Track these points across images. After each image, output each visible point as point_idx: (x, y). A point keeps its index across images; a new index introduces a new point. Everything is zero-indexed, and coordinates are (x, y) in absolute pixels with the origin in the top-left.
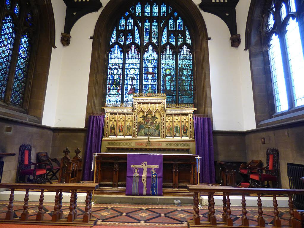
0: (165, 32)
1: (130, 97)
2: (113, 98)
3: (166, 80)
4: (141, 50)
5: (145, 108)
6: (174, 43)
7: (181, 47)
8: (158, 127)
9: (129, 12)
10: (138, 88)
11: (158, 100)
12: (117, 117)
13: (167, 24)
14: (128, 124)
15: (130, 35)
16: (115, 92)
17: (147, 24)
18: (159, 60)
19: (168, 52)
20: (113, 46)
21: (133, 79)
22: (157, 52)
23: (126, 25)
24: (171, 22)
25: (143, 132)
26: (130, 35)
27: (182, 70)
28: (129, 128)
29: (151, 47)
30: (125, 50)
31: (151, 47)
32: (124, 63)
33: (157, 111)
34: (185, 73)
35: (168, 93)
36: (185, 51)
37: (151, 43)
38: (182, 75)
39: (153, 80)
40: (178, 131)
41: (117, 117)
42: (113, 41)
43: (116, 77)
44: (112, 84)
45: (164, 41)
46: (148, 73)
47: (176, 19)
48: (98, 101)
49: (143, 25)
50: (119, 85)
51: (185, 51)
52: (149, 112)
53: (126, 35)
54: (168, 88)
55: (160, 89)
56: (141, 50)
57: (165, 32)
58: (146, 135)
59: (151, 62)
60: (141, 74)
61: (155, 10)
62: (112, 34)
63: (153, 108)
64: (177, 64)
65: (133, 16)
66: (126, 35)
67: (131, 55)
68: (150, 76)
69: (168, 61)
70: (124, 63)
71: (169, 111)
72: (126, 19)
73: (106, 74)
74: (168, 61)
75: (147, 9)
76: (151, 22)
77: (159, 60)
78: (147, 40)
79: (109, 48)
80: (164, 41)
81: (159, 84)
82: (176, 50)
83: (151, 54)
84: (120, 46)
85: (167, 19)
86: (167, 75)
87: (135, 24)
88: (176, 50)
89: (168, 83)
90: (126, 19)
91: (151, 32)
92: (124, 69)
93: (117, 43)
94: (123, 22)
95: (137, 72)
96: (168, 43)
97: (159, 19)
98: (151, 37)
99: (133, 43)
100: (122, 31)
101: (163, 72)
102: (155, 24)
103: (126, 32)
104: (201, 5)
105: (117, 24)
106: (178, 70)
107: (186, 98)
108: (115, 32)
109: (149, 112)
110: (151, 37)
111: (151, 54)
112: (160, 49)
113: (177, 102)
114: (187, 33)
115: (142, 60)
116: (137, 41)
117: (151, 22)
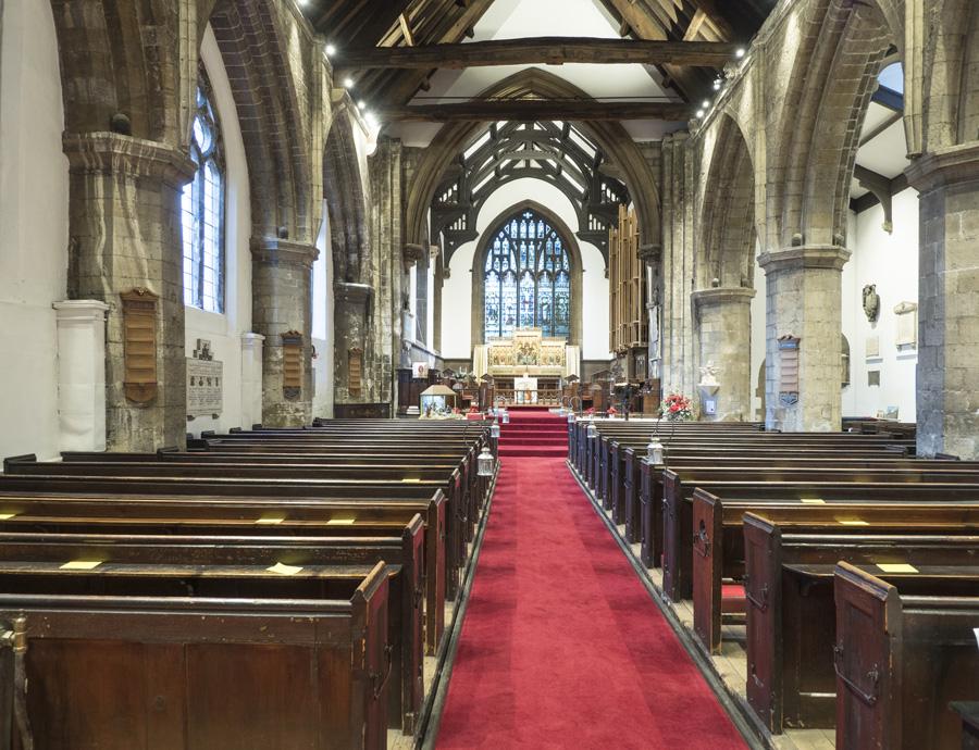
0: (542, 257)
1: (509, 328)
2: (492, 328)
3: (542, 310)
5: (524, 341)
6: (551, 270)
7: (558, 274)
8: (535, 358)
9: (505, 233)
10: (515, 317)
11: (534, 333)
12: (500, 349)
13: (544, 247)
14: (510, 354)
15: (505, 261)
16: (493, 322)
17: (523, 247)
18: (536, 288)
19: (545, 280)
20: (488, 273)
21: (510, 308)
22: (533, 279)
23: (501, 249)
24: (549, 244)
25: (522, 361)
26: (505, 261)
27: (559, 298)
28: (510, 359)
29: (527, 273)
30: (501, 276)
31: (527, 273)
32: (501, 292)
33: (534, 344)
34: (561, 301)
35: (545, 322)
36: (562, 278)
37: (527, 269)
38: (558, 304)
39: (530, 309)
40: (552, 360)
41: (500, 349)
42: (488, 267)
43: (494, 307)
44: (490, 313)
45: (541, 267)
46: (525, 302)
47: (553, 241)
48: (479, 332)
49: (519, 248)
50: (496, 314)
51: (562, 278)
52: (527, 344)
53: (501, 261)
54: (545, 317)
55: (536, 321)
56: (518, 277)
57: (542, 257)
58: (525, 364)
59: (528, 290)
60: (518, 304)
61: (532, 229)
62: (486, 258)
63: (530, 341)
64: (553, 293)
65: (508, 236)
66: (501, 261)
68: (527, 306)
69: (545, 290)
70: (501, 292)
71: (544, 343)
72: (501, 240)
73: (483, 304)
74: (545, 290)
75: (523, 229)
76: (527, 244)
77: (536, 288)
78: (523, 266)
79: (485, 275)
80: (541, 267)
81: (536, 315)
82: (553, 277)
83: (527, 281)
84: (497, 273)
85: (545, 241)
86: (543, 304)
87: (511, 247)
88: (553, 277)
89: (544, 313)
90: (501, 240)
91: (528, 257)
92: (501, 298)
93: (493, 269)
94: (497, 244)
95: (515, 301)
96: (545, 270)
97: (536, 241)
98: (527, 262)
99: (509, 269)
100: (497, 256)
102: (532, 247)
103: (501, 257)
104: (577, 234)
105: (492, 247)
106: (555, 299)
107: (561, 328)
108: (490, 257)
109: (527, 344)
110: (527, 262)
111: (527, 281)
112: (536, 276)
113: (553, 335)
114: (565, 257)
115: (518, 288)
116: (514, 267)
117: (527, 244)
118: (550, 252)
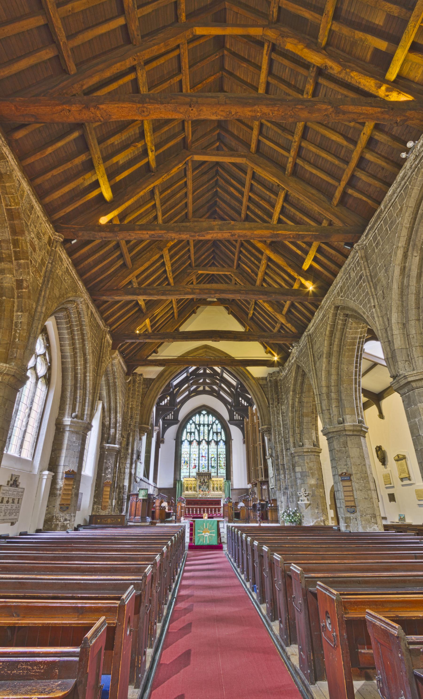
4: (199, 443)
19: (213, 444)
20: (184, 441)
27: (220, 454)
30: (190, 443)
34: (221, 456)
37: (204, 439)
46: (202, 456)
56: (199, 443)
67: (193, 447)
74: (213, 450)
79: (182, 442)
80: (211, 438)
82: (217, 443)
84: (188, 441)
92: (190, 454)
96: (213, 439)
101: (210, 457)
112: (208, 443)
118: (215, 430)
